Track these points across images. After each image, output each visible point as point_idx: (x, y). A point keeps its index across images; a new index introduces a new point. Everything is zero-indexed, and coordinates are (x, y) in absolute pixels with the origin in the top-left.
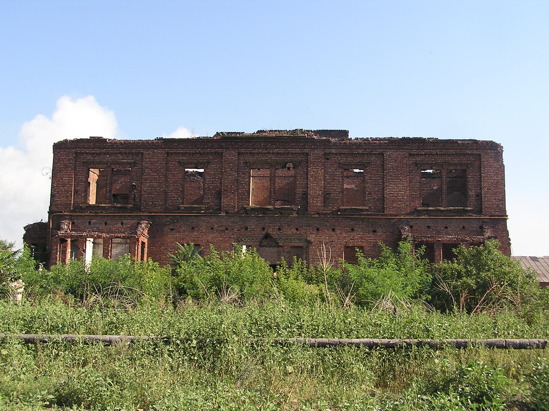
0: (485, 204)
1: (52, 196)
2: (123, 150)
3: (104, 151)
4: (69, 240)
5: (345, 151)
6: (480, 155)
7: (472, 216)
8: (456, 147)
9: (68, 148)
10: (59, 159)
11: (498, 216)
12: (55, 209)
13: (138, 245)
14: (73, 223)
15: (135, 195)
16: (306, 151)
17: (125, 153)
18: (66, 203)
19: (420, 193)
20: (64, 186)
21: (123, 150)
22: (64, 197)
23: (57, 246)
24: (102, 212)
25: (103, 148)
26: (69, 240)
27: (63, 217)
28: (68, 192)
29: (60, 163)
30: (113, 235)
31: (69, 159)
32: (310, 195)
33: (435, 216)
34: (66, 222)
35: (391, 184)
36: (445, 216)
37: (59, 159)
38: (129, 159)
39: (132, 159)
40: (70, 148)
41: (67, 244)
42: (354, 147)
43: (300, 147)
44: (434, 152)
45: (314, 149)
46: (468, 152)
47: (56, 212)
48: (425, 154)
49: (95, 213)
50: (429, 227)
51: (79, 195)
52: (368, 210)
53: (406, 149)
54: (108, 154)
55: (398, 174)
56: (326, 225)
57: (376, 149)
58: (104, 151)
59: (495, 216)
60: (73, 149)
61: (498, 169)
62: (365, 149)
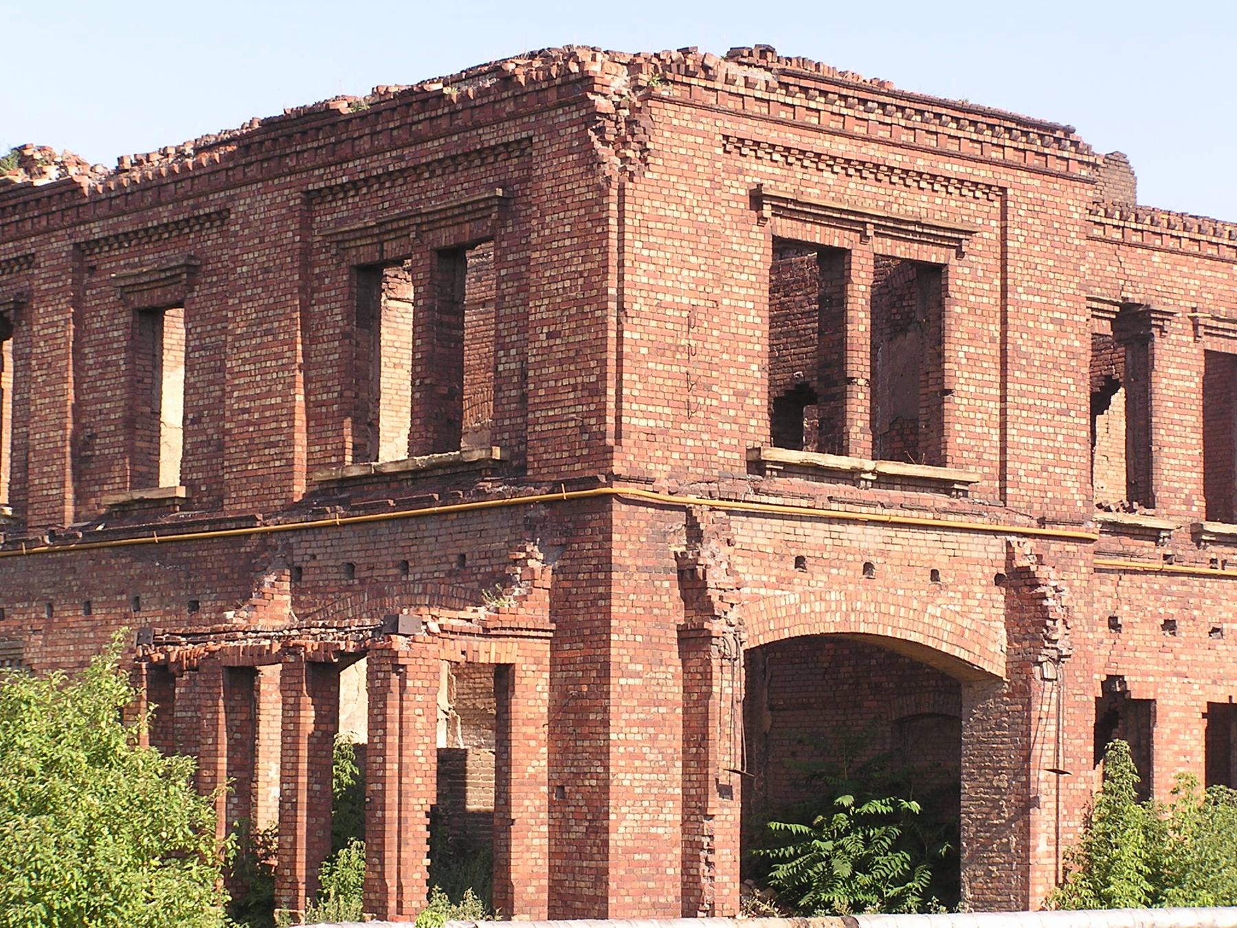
0: (541, 422)
5: (127, 224)
6: (530, 139)
7: (482, 494)
8: (444, 123)
11: (570, 484)
16: (29, 245)
19: (341, 395)
32: (34, 451)
33: (368, 509)
35: (246, 361)
36: (400, 505)
42: (149, 197)
43: (12, 231)
44: (376, 166)
45: (48, 230)
46: (490, 137)
48: (355, 185)
50: (351, 567)
52: (186, 504)
53: (290, 174)
55: (267, 308)
56: (70, 587)
57: (207, 195)
59: (556, 487)
61: (587, 205)
62: (177, 201)
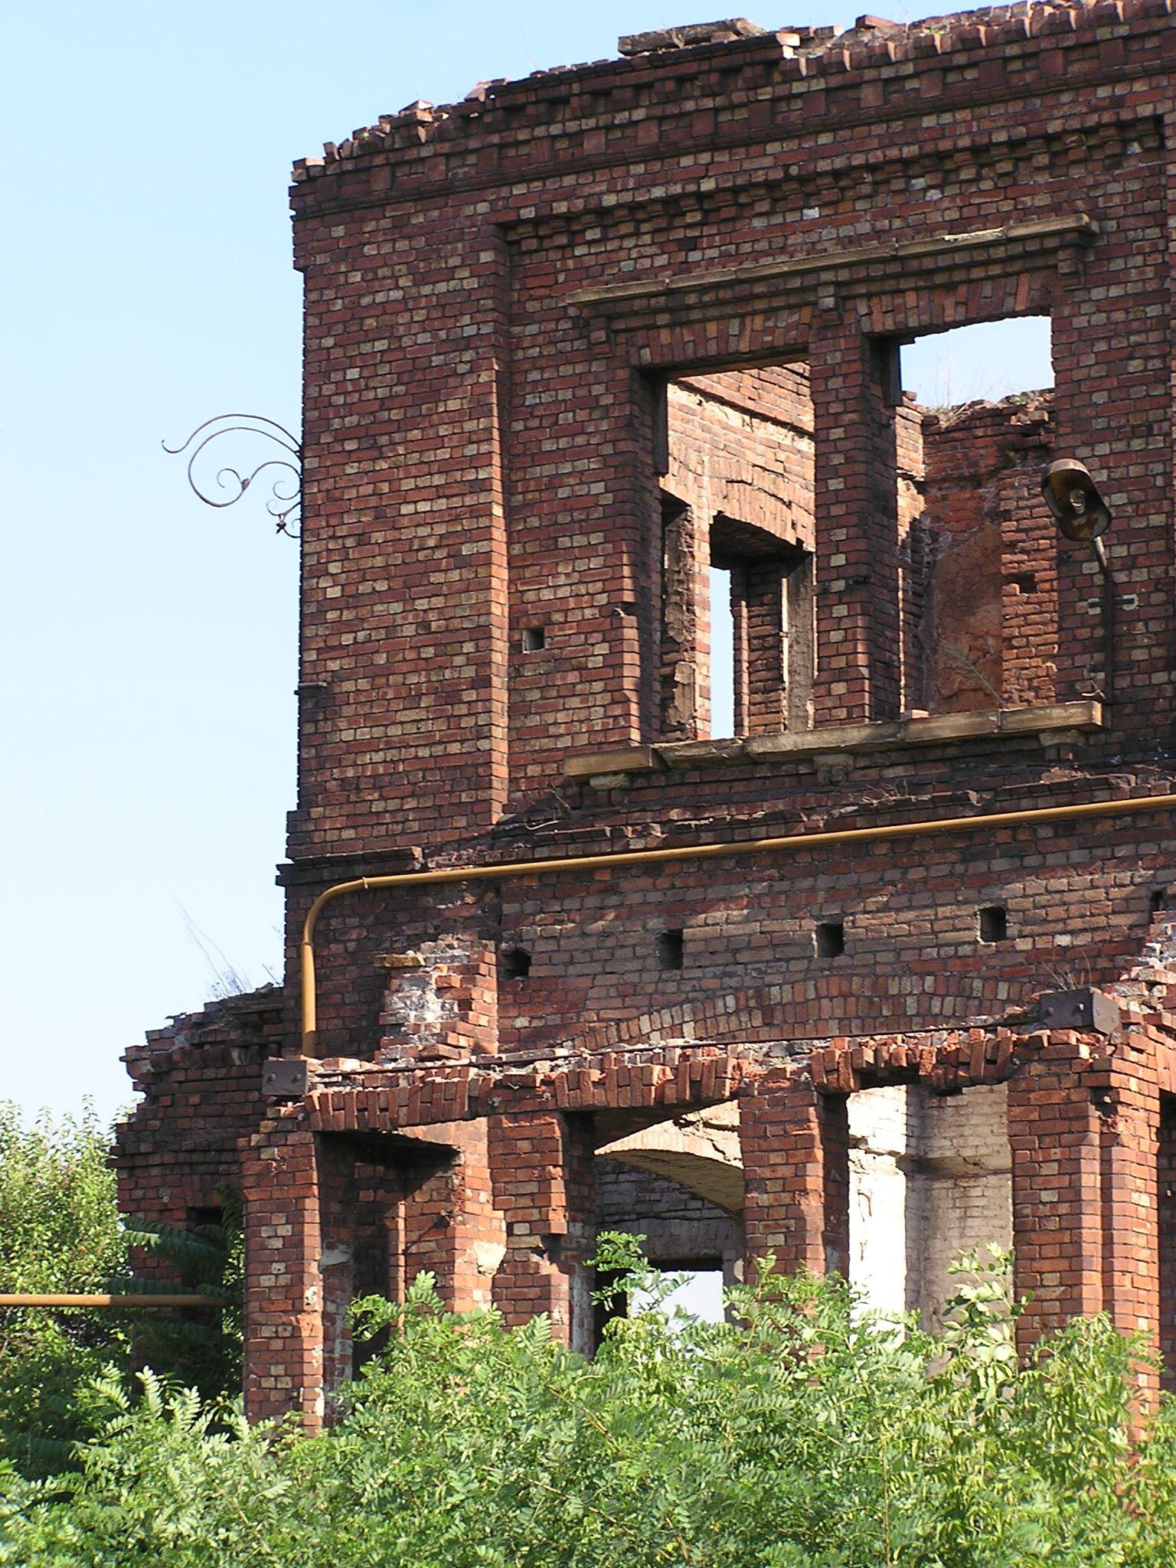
1: (315, 701)
2: (960, 128)
3: (764, 163)
4: (470, 1141)
9: (423, 196)
10: (355, 313)
12: (339, 834)
13: (1110, 1139)
14: (515, 966)
15: (1111, 595)
17: (979, 151)
18: (439, 763)
20: (410, 581)
21: (960, 128)
22: (413, 698)
23: (297, 1220)
24: (784, 821)
25: (754, 141)
26: (470, 1141)
27: (414, 911)
28: (446, 643)
29: (367, 362)
30: (841, 1047)
31: (442, 304)
34: (440, 957)
37: (355, 313)
38: (1024, 215)
39: (1056, 209)
40: (446, 190)
41: (451, 1195)
47: (348, 866)
49: (721, 830)
51: (561, 663)
54: (806, 187)
58: (764, 163)
60: (477, 188)
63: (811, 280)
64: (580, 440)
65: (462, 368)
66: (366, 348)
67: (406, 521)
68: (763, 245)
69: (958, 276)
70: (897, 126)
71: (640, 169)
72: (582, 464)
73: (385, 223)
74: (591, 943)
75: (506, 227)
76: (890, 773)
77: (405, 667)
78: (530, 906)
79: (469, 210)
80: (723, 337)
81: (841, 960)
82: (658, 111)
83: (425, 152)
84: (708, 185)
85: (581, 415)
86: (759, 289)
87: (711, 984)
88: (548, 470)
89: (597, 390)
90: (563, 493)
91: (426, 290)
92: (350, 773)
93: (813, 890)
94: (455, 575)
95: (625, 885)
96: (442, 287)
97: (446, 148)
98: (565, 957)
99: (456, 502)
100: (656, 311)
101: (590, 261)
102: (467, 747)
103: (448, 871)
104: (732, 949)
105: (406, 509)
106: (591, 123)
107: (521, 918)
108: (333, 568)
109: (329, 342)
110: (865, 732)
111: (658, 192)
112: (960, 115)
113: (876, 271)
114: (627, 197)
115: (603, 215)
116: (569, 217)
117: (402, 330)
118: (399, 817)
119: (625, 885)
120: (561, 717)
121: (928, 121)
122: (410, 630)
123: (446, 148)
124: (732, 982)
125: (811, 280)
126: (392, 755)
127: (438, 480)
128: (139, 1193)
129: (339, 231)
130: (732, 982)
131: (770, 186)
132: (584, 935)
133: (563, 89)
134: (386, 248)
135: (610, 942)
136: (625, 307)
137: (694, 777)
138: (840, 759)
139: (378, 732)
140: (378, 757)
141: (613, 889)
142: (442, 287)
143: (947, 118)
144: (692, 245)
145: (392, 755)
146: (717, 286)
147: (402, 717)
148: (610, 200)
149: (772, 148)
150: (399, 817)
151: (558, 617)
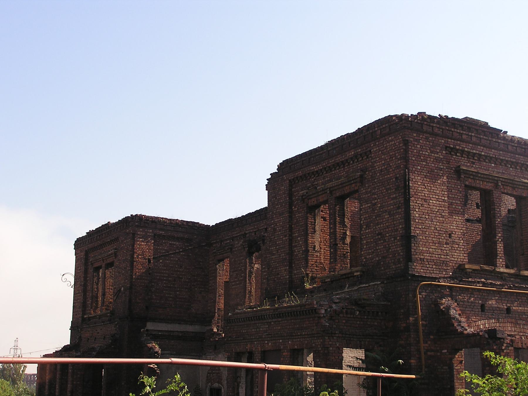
3: (492, 153)
9: (433, 134)
40: (437, 135)
63: (499, 179)
64: (456, 196)
65: (440, 174)
66: (421, 163)
67: (431, 204)
68: (485, 168)
69: (520, 187)
70: (512, 155)
71: (471, 145)
72: (457, 202)
73: (424, 137)
74: (470, 304)
75: (446, 147)
76: (512, 279)
77: (432, 236)
78: (458, 294)
79: (440, 141)
80: (479, 184)
81: (510, 315)
82: (476, 135)
83: (435, 125)
84: (483, 154)
85: (456, 191)
86: (491, 177)
87: (491, 316)
88: (451, 201)
89: (459, 187)
90: (454, 206)
91: (433, 155)
92: (422, 257)
93: (505, 300)
94: (441, 219)
95: (475, 293)
96: (436, 155)
97: (438, 126)
98: (465, 306)
99: (441, 203)
100: (471, 175)
101: (456, 159)
102: (445, 257)
103: (444, 284)
104: (493, 310)
105: (431, 201)
106: (465, 132)
107: (456, 296)
108: (417, 210)
109: (414, 159)
110: (514, 271)
111: (474, 151)
112: (522, 157)
113: (509, 181)
114: (469, 150)
115: (463, 152)
116: (458, 150)
117: (428, 162)
118: (432, 269)
119: (475, 293)
120: (455, 254)
121: (517, 156)
122: (433, 228)
123: (438, 126)
124: (494, 316)
125: (499, 179)
126: (430, 255)
127: (437, 197)
128: (331, 343)
129: (415, 135)
130: (494, 316)
131: (491, 158)
132: (468, 302)
133: (464, 124)
134: (424, 142)
135: (473, 305)
136: (468, 172)
137: (476, 272)
138: (507, 275)
139: (427, 249)
140: (428, 255)
141: (472, 293)
142: (436, 155)
143: (519, 156)
144: (473, 163)
145: (430, 255)
146: (473, 172)
147: (432, 247)
148: (466, 149)
149: (493, 150)
150: (432, 269)
151: (454, 232)
